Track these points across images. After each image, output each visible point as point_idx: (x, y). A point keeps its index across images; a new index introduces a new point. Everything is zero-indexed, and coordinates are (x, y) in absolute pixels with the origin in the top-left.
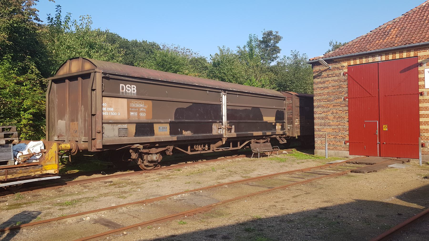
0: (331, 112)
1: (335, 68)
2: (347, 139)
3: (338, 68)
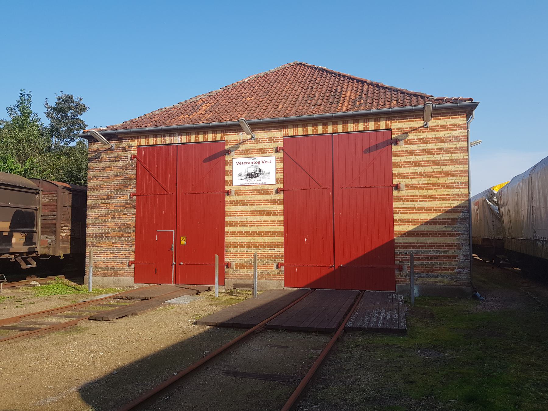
0: (111, 216)
2: (132, 258)
3: (124, 149)
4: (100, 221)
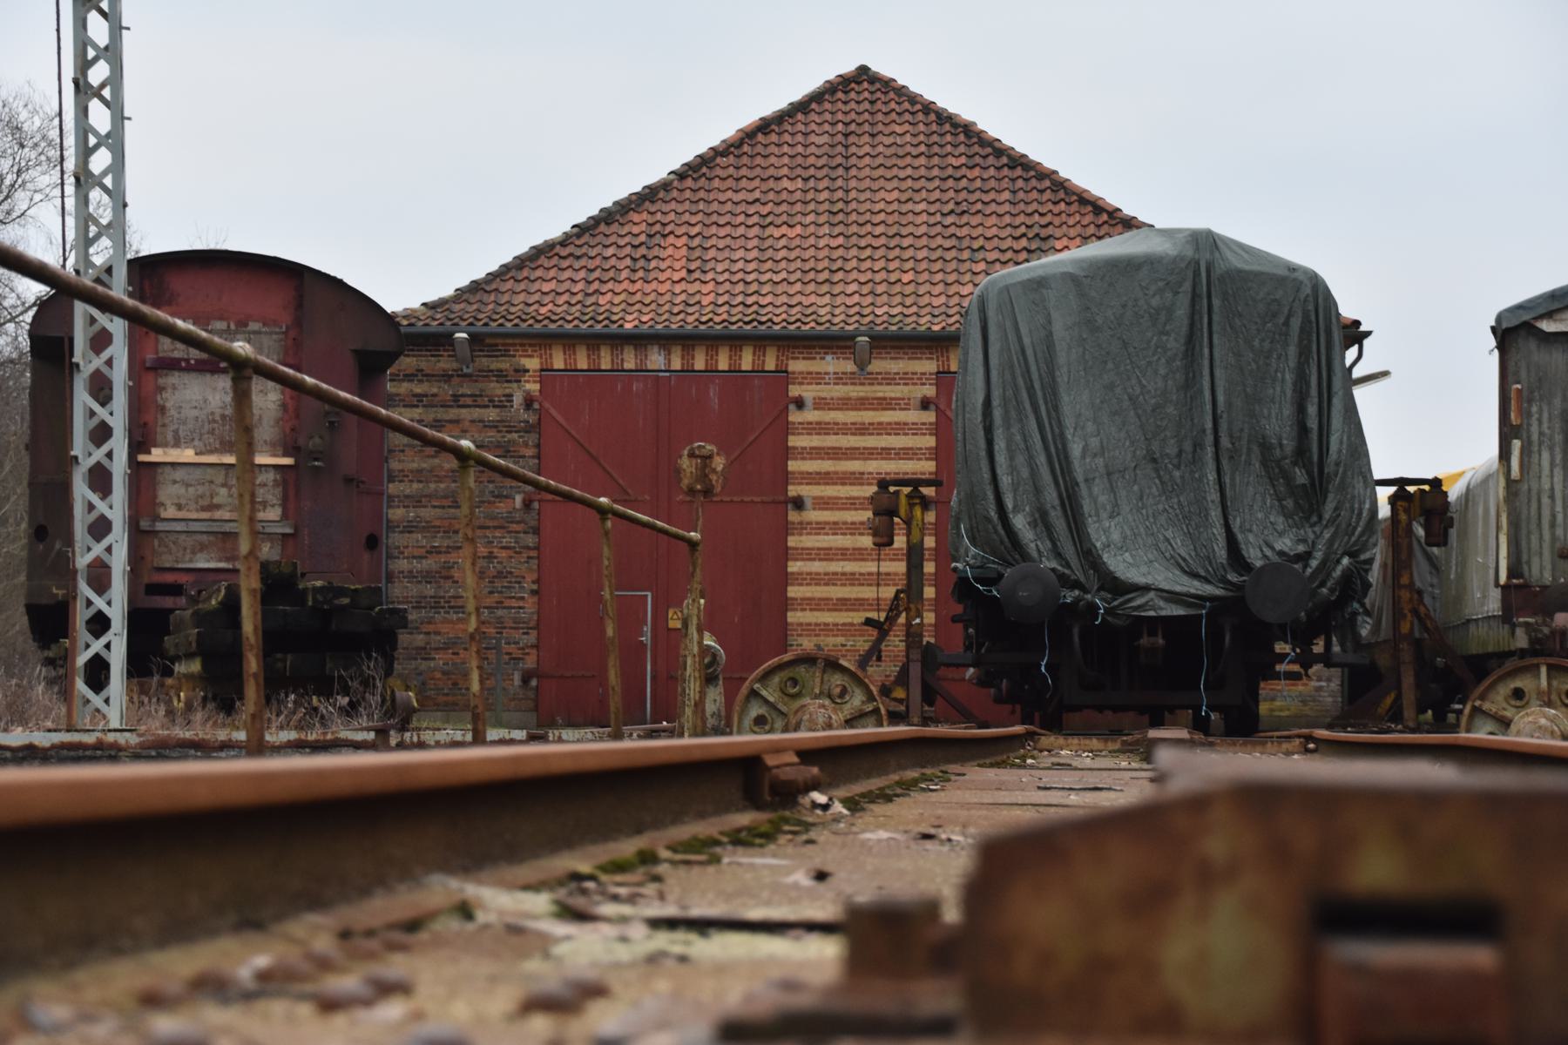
1: (487, 374)
3: (501, 376)
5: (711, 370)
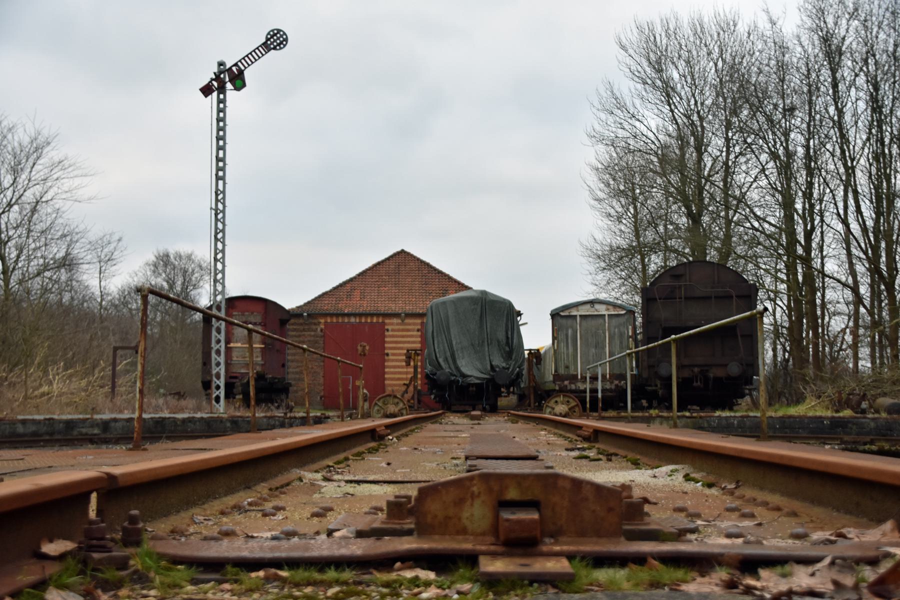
1: (311, 323)
3: (315, 324)
4: (298, 370)
5: (366, 322)
